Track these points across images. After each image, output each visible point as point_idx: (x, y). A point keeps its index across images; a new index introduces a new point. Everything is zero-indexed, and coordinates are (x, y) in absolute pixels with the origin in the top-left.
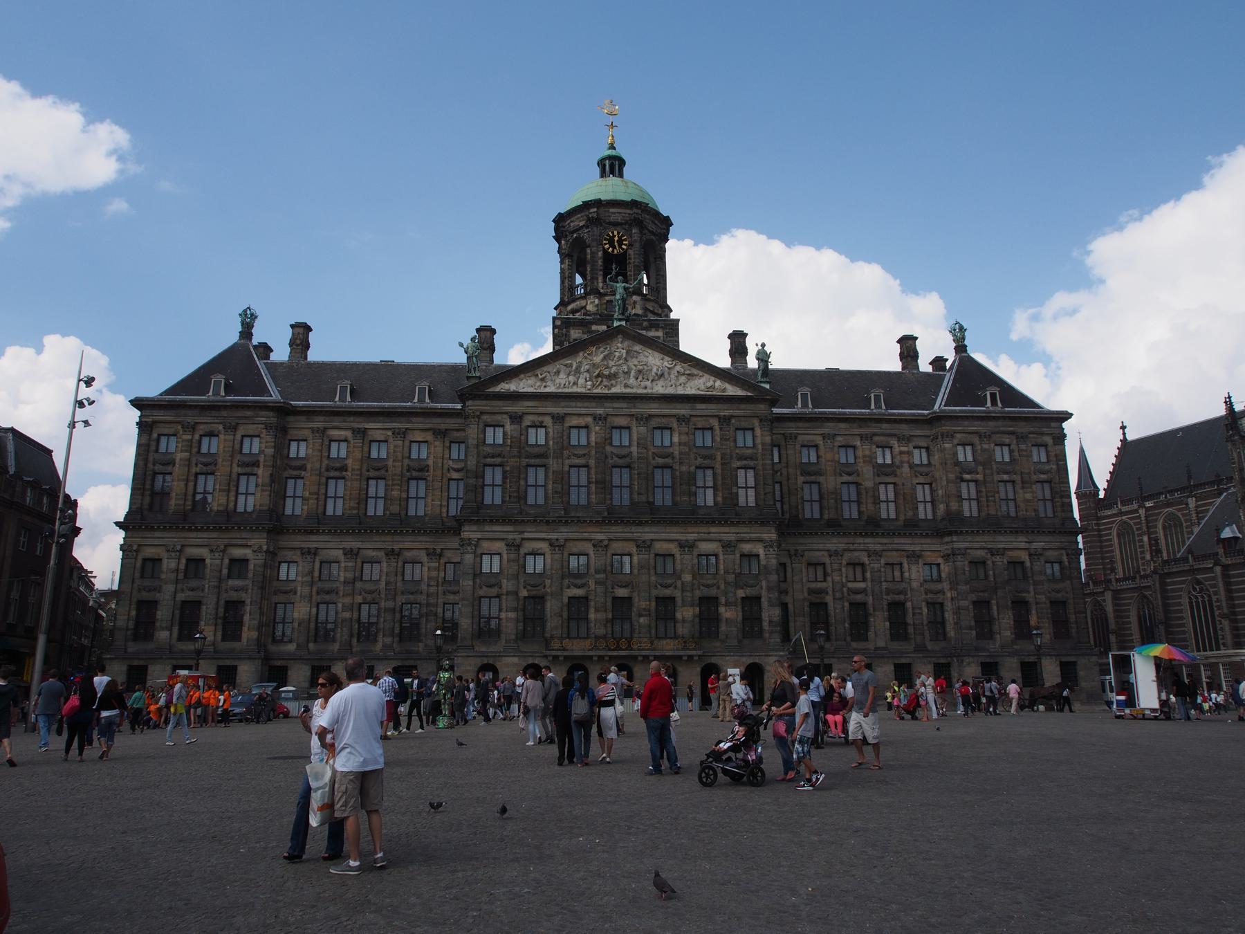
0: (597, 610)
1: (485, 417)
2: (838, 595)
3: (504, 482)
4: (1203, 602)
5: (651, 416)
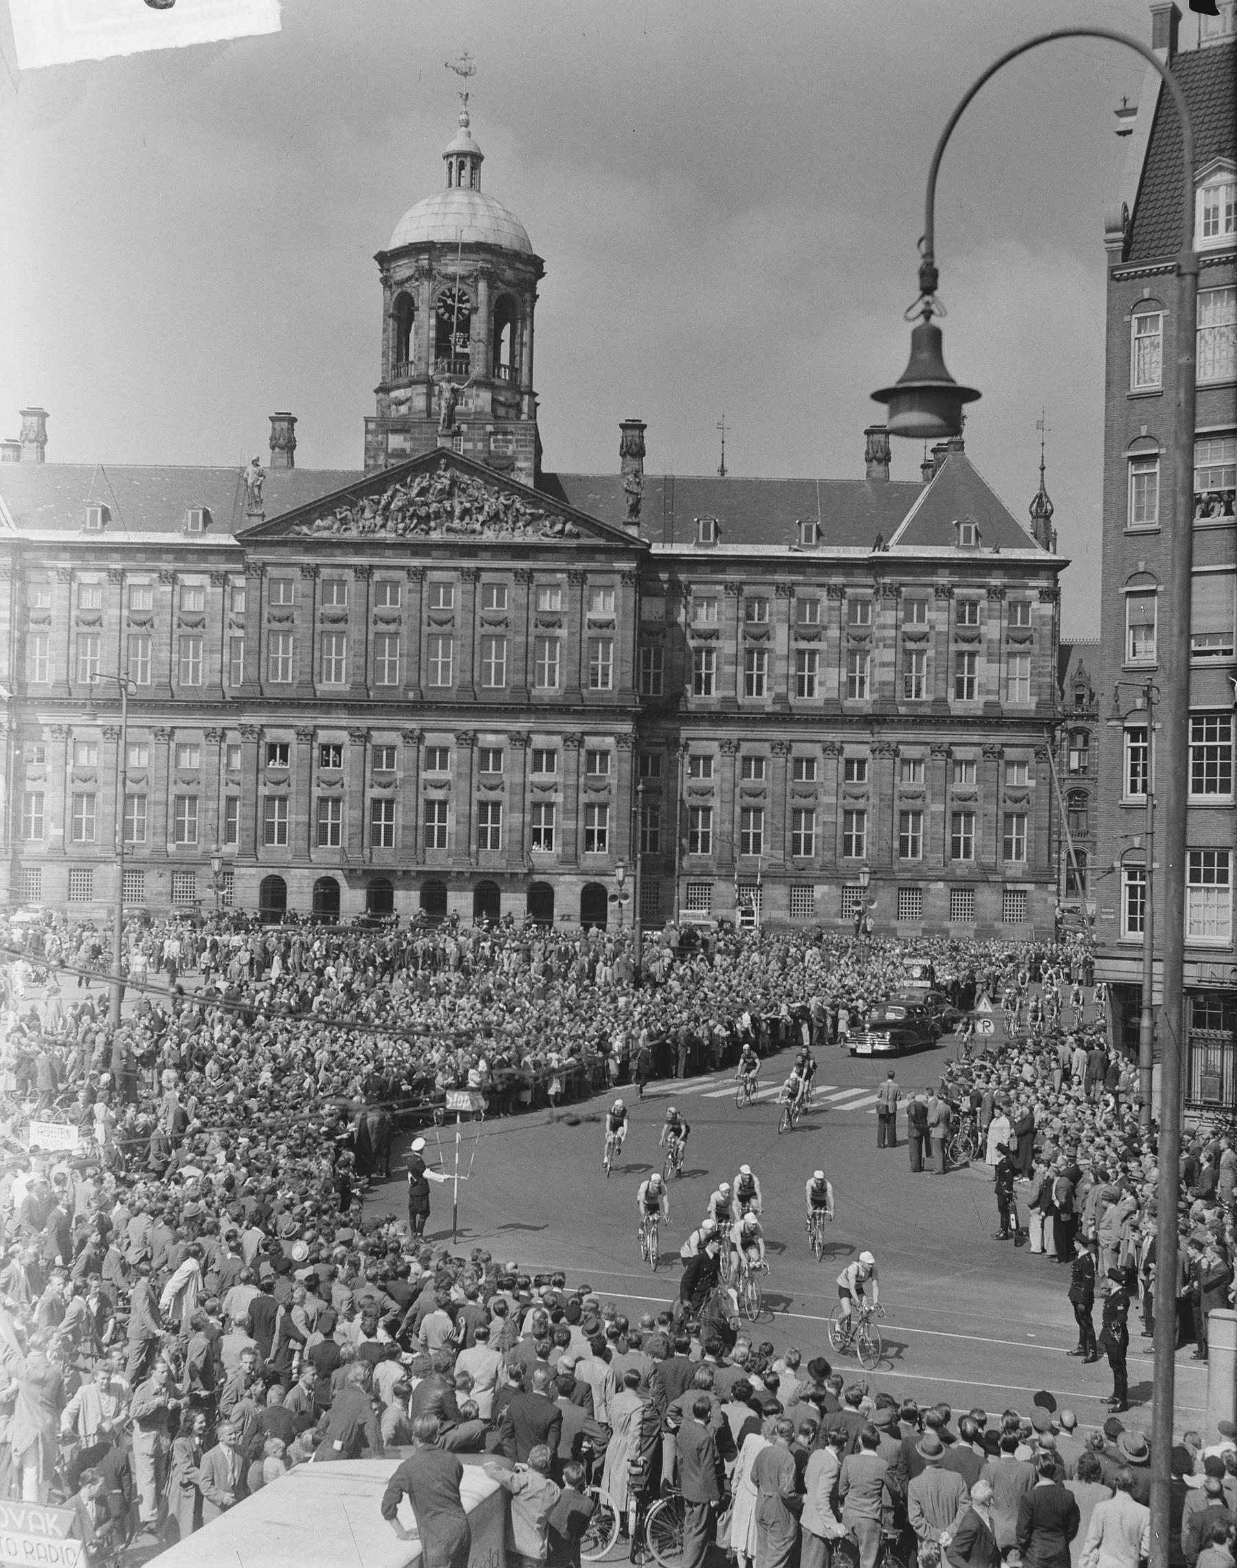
0: (405, 814)
2: (728, 797)
5: (479, 569)
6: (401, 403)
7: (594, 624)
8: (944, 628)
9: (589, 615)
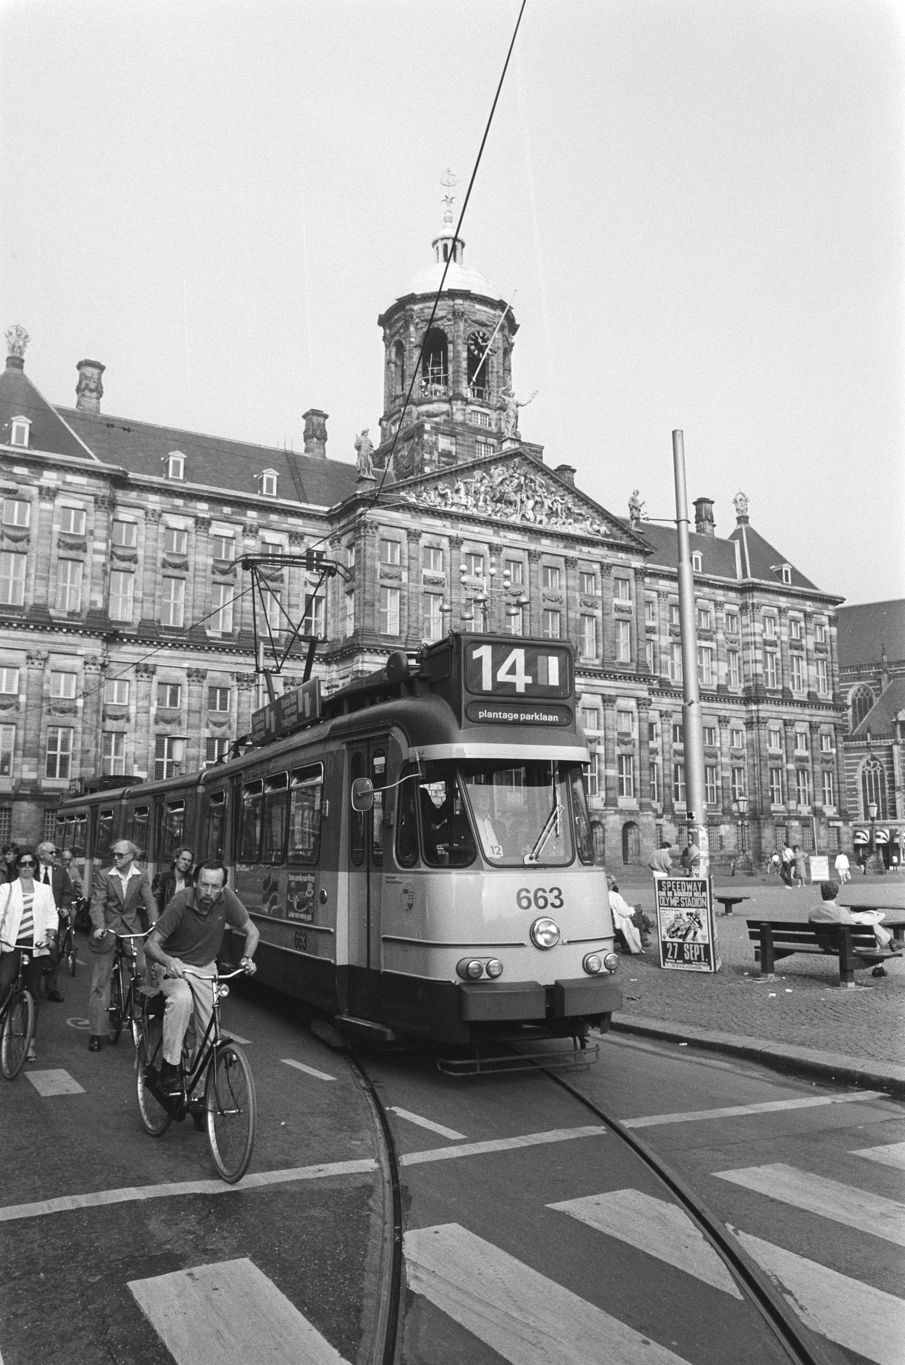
1: (381, 528)
2: (667, 756)
3: (401, 610)
4: (876, 776)
6: (436, 415)
7: (619, 609)
8: (785, 638)
9: (616, 601)
